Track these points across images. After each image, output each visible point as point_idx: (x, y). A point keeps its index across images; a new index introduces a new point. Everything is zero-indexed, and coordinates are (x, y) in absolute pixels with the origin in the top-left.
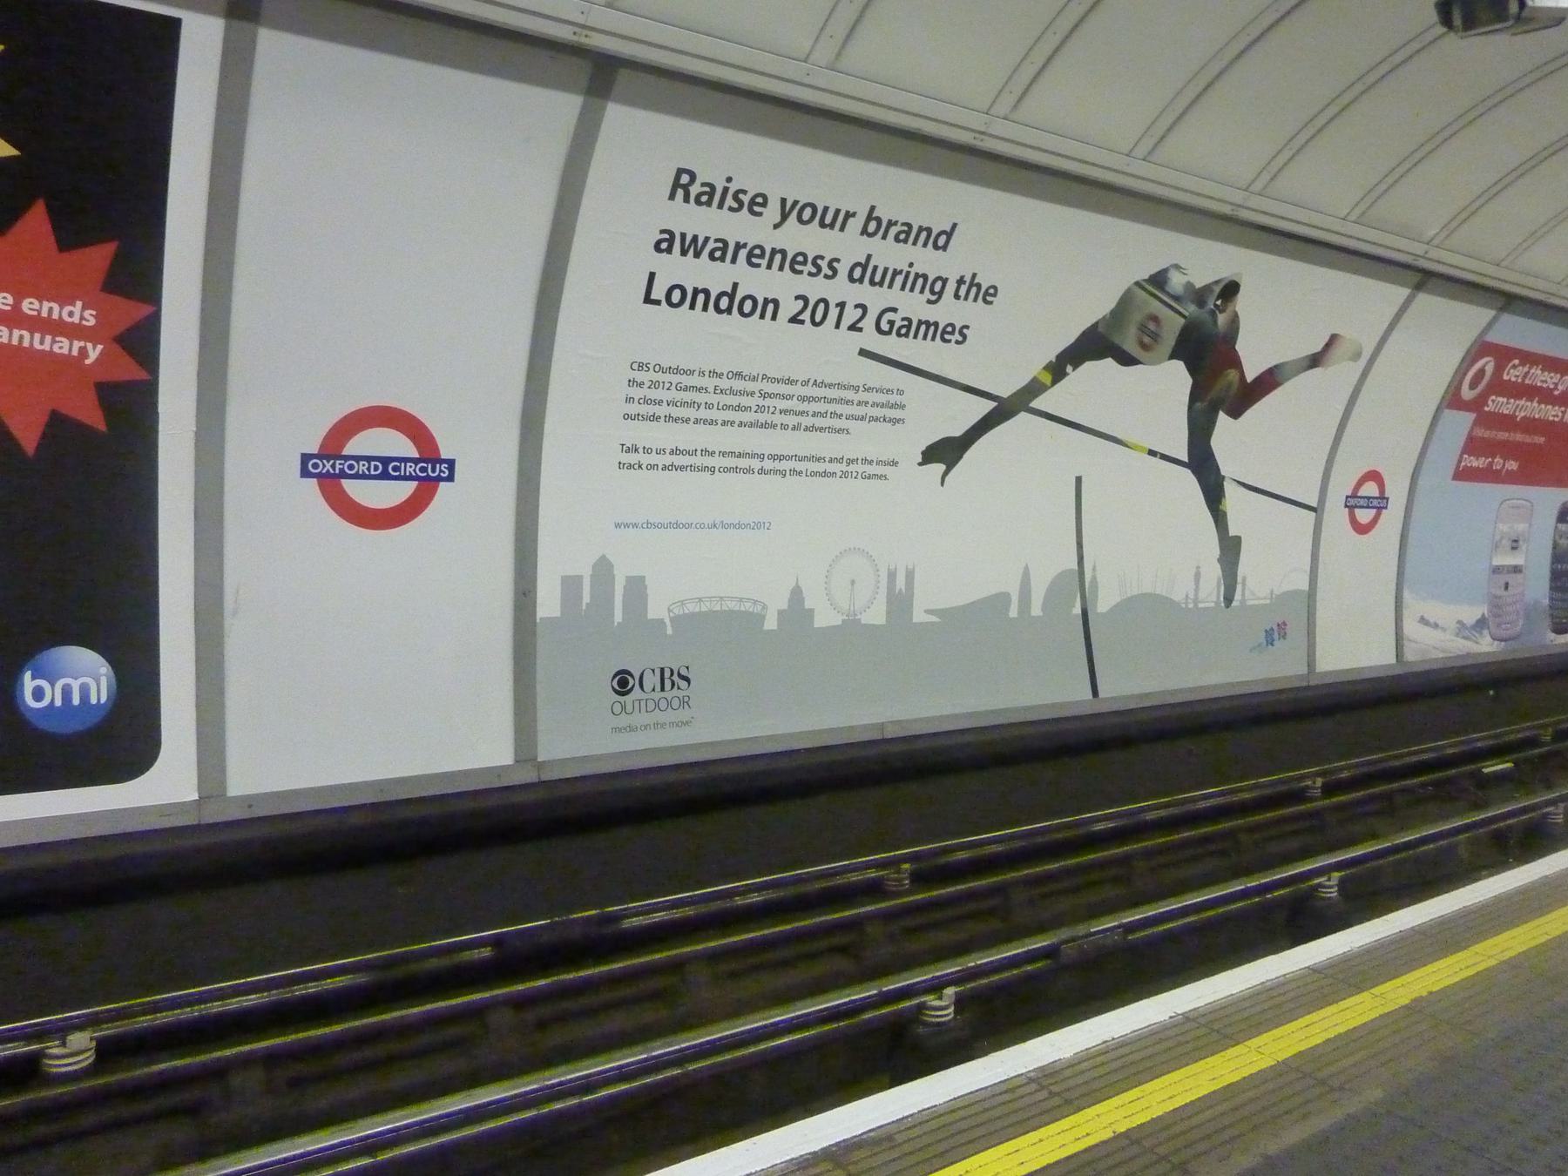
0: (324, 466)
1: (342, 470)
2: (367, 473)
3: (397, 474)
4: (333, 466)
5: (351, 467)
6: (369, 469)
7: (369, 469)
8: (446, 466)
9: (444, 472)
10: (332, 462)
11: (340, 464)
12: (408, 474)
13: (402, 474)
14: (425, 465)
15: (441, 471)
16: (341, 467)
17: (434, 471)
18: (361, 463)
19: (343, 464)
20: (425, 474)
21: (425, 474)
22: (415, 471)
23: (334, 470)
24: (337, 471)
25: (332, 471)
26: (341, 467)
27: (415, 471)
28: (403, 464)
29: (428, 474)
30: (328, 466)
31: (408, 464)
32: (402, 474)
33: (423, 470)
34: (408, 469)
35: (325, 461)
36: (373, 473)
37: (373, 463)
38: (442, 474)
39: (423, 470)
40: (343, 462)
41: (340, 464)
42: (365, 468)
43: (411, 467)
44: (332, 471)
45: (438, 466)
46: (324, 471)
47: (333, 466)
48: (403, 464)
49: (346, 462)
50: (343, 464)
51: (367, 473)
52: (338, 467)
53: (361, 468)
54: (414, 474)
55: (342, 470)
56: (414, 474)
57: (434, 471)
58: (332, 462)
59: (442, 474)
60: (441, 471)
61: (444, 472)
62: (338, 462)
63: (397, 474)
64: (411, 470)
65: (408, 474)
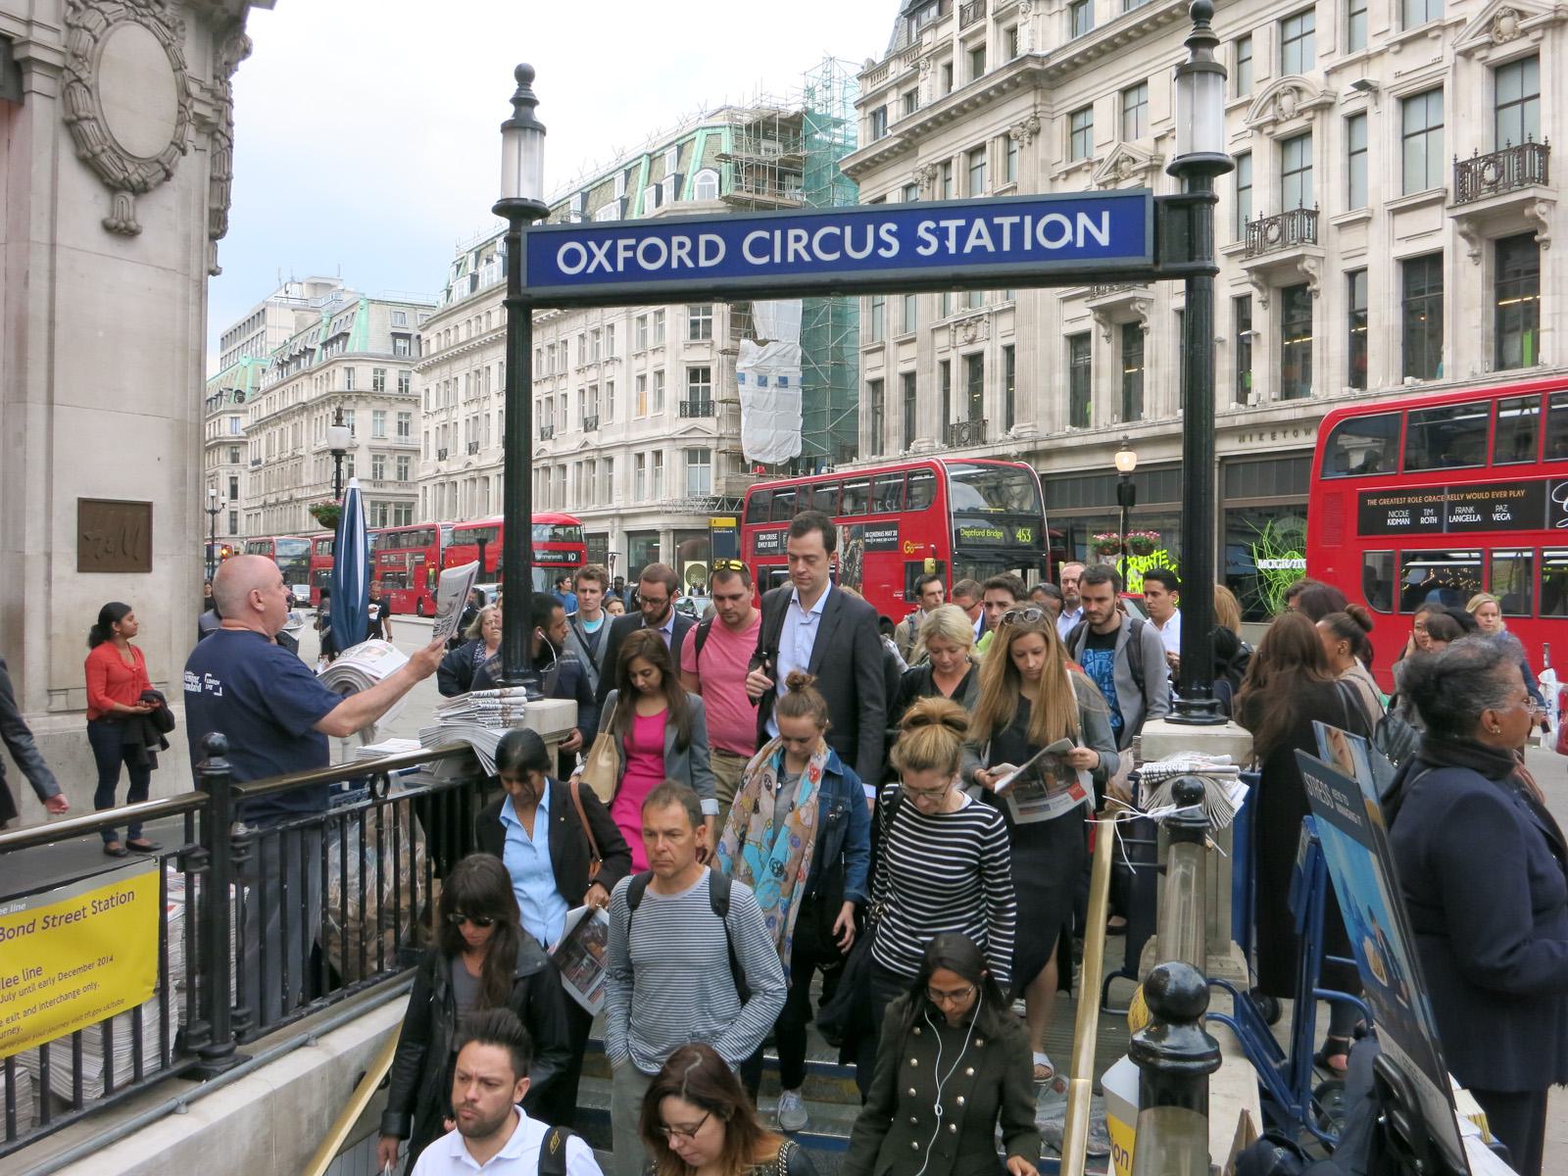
0: (591, 256)
2: (690, 264)
3: (765, 260)
4: (611, 256)
5: (652, 253)
6: (694, 254)
7: (694, 254)
8: (893, 227)
9: (888, 247)
10: (608, 244)
11: (627, 248)
12: (791, 258)
13: (778, 259)
16: (630, 254)
17: (859, 245)
18: (675, 240)
19: (633, 248)
20: (836, 256)
21: (836, 256)
22: (809, 248)
23: (614, 264)
24: (620, 267)
25: (608, 268)
26: (630, 254)
27: (809, 248)
28: (778, 234)
29: (844, 254)
30: (600, 256)
31: (792, 233)
32: (778, 259)
33: (831, 243)
34: (792, 246)
35: (592, 245)
36: (703, 263)
37: (703, 239)
38: (883, 252)
39: (831, 243)
40: (632, 242)
41: (627, 248)
42: (683, 253)
43: (798, 239)
44: (608, 268)
45: (870, 229)
46: (591, 270)
47: (611, 256)
48: (778, 234)
49: (638, 242)
50: (633, 248)
51: (690, 264)
52: (622, 255)
53: (676, 252)
54: (806, 258)
56: (806, 258)
57: (859, 245)
58: (608, 244)
59: (883, 252)
60: (879, 243)
61: (888, 247)
62: (621, 243)
63: (765, 260)
64: (800, 247)
65: (791, 258)
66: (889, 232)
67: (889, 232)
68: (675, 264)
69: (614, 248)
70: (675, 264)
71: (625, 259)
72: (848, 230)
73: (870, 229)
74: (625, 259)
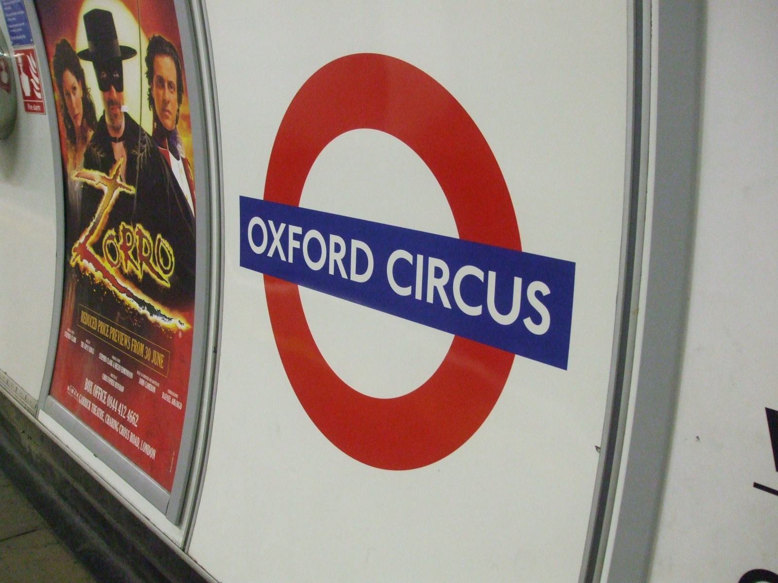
1: (298, 252)
4: (284, 241)
8: (546, 290)
9: (537, 319)
13: (419, 296)
14: (479, 274)
15: (527, 310)
16: (297, 244)
17: (504, 307)
20: (475, 311)
22: (449, 288)
26: (297, 244)
27: (449, 288)
28: (420, 258)
29: (485, 310)
32: (419, 296)
34: (432, 281)
40: (299, 230)
45: (518, 282)
47: (284, 241)
48: (420, 258)
52: (293, 244)
55: (298, 252)
56: (447, 304)
57: (504, 307)
58: (283, 226)
60: (527, 310)
61: (537, 319)
65: (430, 299)
66: (538, 294)
67: (538, 294)
68: (331, 271)
69: (286, 231)
70: (331, 271)
71: (294, 249)
72: (492, 275)
73: (518, 282)
74: (294, 249)
